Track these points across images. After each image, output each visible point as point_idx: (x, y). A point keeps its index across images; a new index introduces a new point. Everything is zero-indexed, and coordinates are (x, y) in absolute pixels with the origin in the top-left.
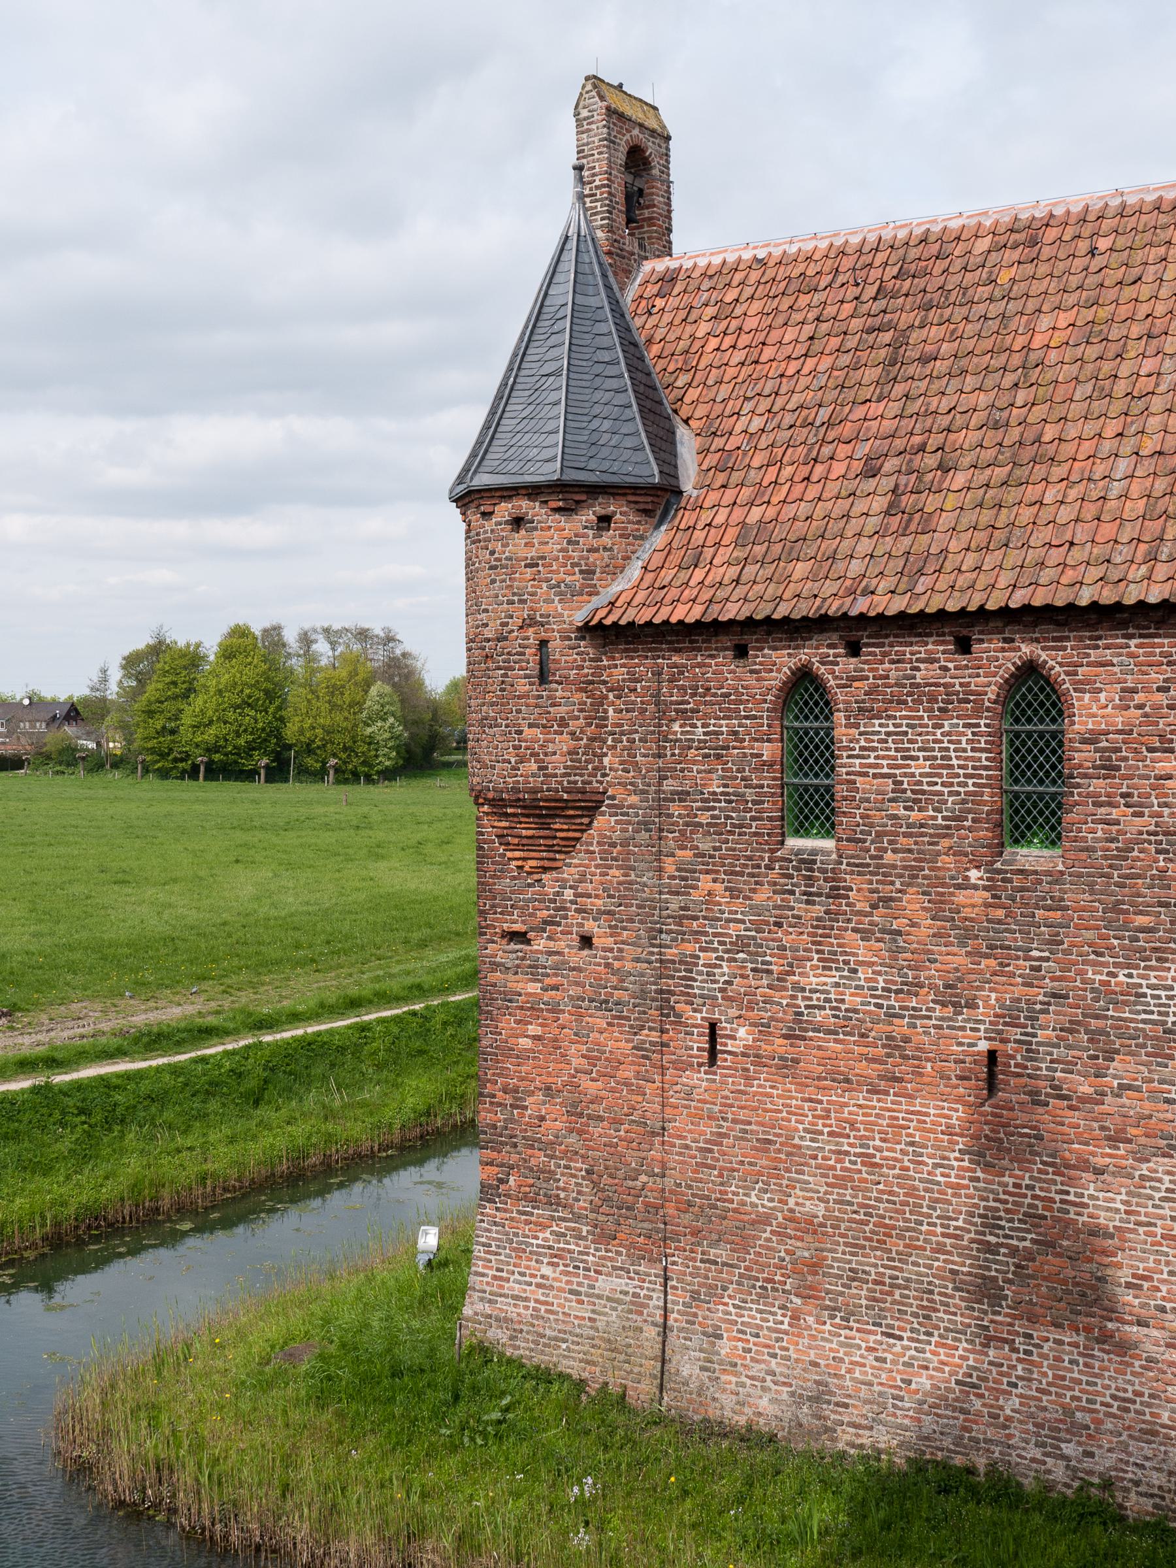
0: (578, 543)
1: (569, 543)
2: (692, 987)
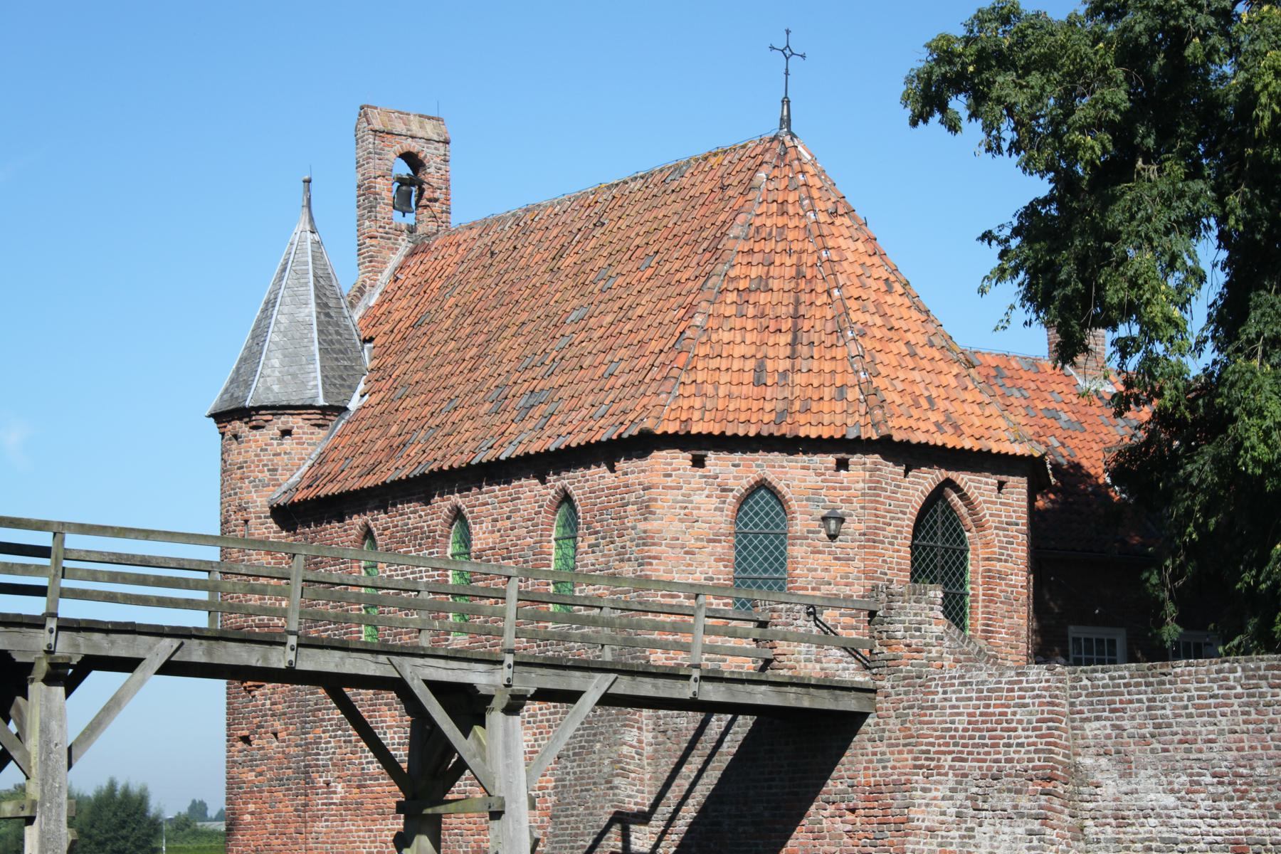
0: (266, 450)
1: (262, 450)
2: (318, 760)
